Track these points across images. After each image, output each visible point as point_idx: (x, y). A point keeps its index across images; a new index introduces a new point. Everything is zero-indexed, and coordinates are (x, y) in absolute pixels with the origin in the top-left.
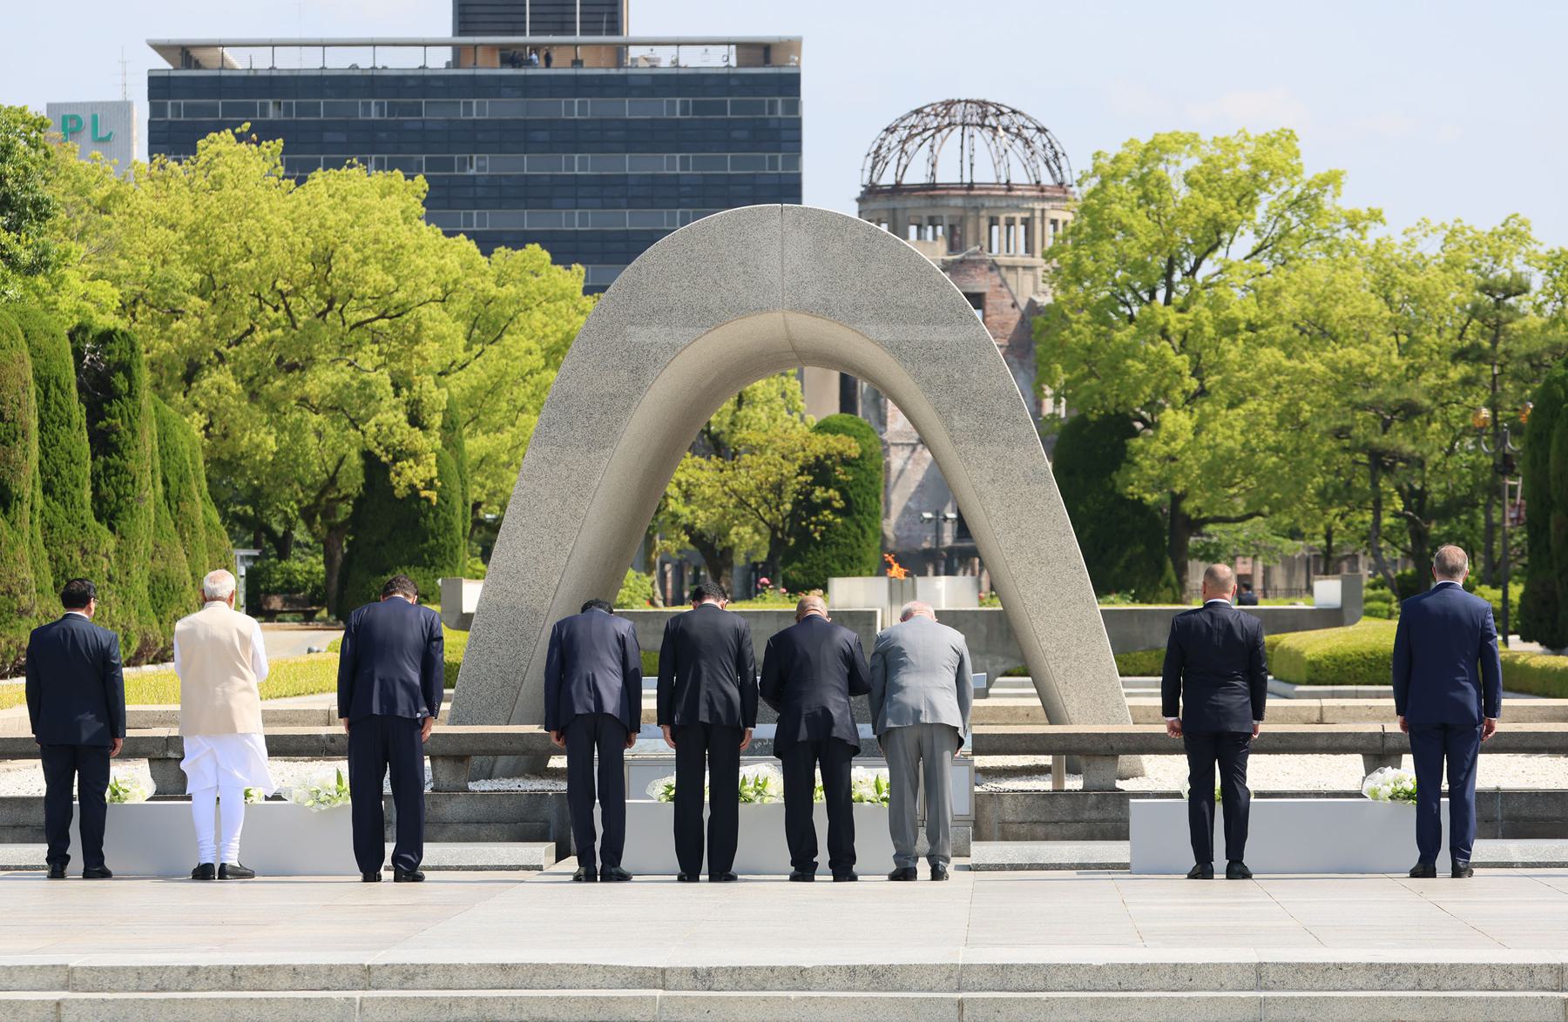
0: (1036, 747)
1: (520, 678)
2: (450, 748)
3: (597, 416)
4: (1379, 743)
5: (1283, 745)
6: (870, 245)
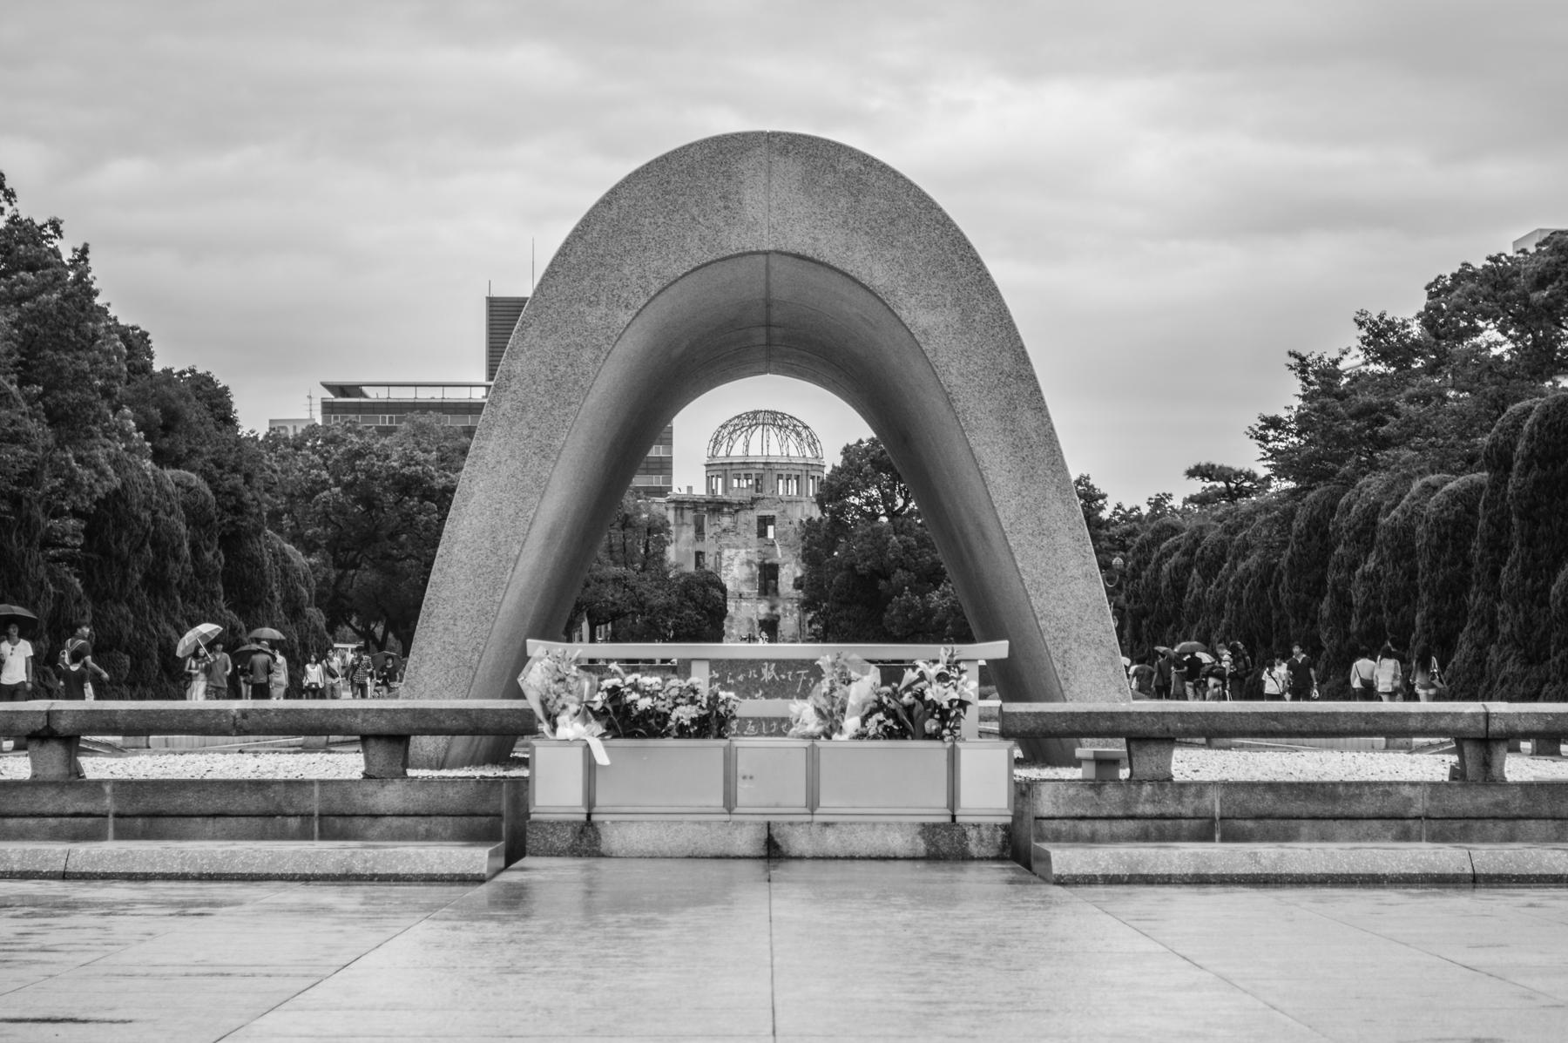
1: (476, 657)
2: (383, 725)
3: (562, 368)
4: (1482, 726)
5: (1369, 727)
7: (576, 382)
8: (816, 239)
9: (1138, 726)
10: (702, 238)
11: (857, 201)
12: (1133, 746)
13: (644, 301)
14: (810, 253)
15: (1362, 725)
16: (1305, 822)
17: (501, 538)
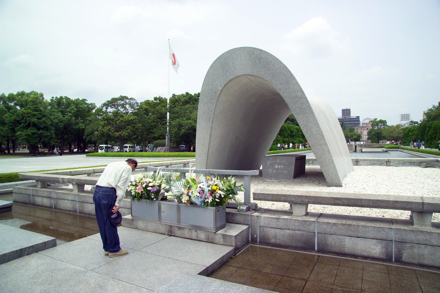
0: (275, 199)
6: (261, 55)
8: (253, 71)
9: (293, 199)
11: (260, 60)
12: (293, 205)
13: (221, 88)
14: (252, 74)
15: (371, 204)
16: (347, 237)
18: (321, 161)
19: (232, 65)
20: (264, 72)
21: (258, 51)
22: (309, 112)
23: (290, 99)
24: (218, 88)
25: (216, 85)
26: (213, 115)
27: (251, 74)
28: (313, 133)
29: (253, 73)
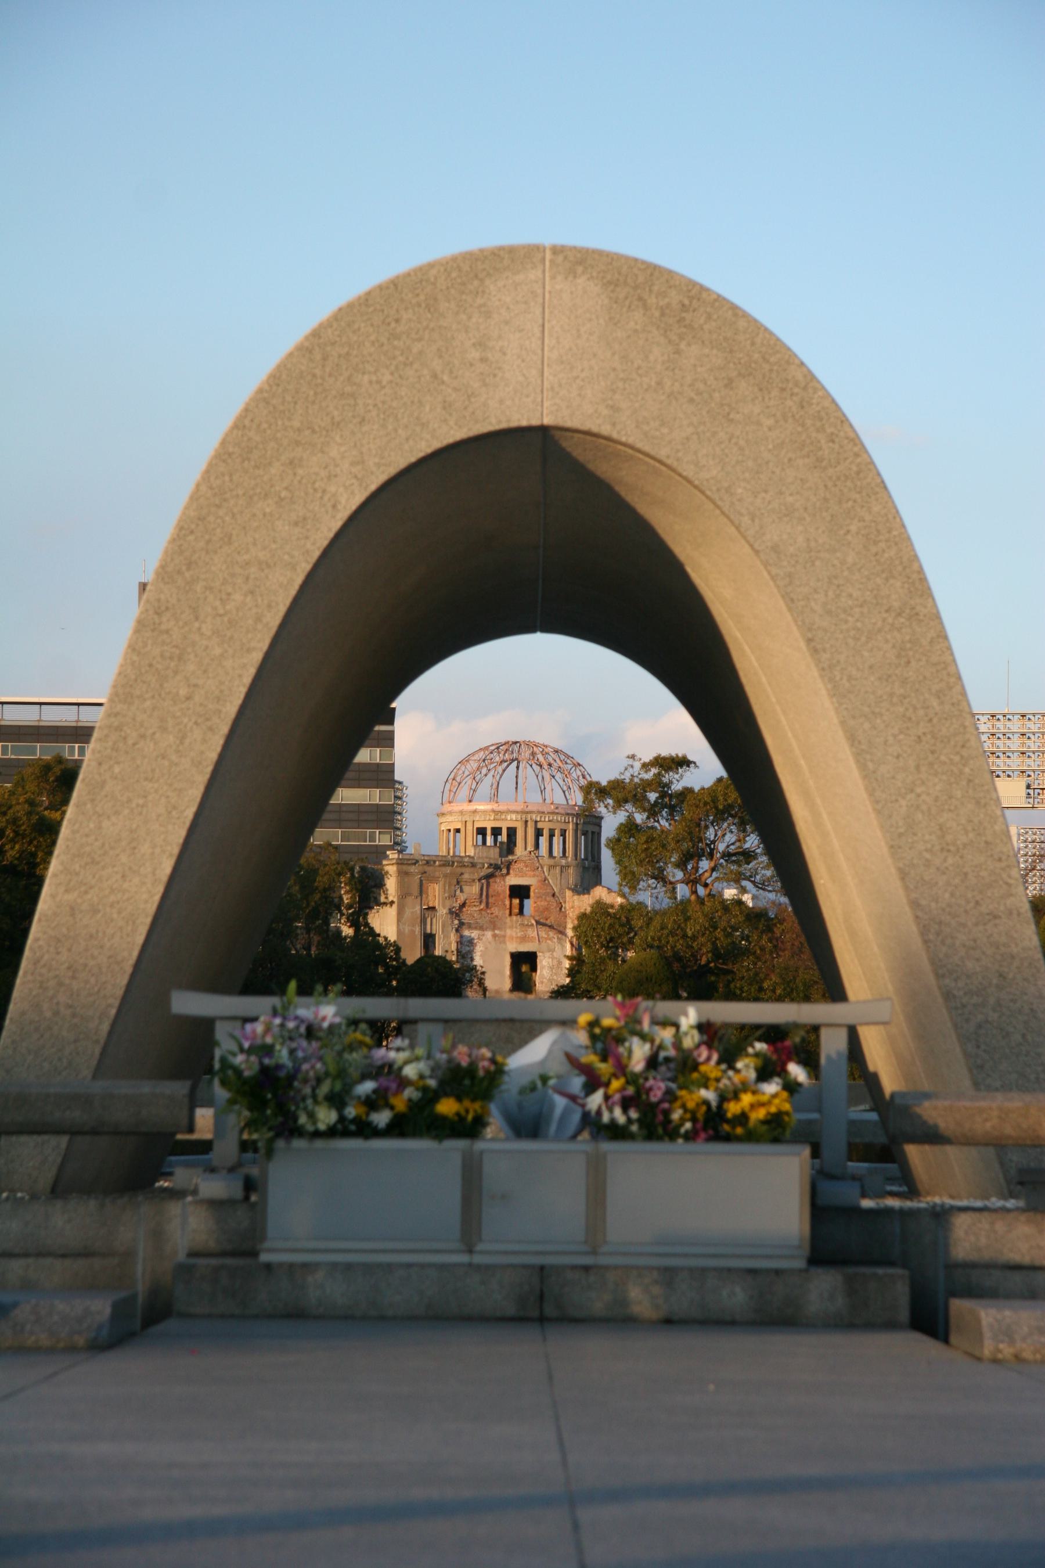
3: (238, 597)
6: (688, 316)
7: (258, 619)
10: (447, 406)
11: (678, 352)
17: (145, 848)
18: (979, 1026)
19: (474, 354)
20: (690, 430)
21: (673, 293)
22: (942, 703)
23: (829, 612)
24: (332, 489)
25: (323, 474)
26: (247, 680)
27: (595, 429)
28: (949, 838)
29: (614, 424)
